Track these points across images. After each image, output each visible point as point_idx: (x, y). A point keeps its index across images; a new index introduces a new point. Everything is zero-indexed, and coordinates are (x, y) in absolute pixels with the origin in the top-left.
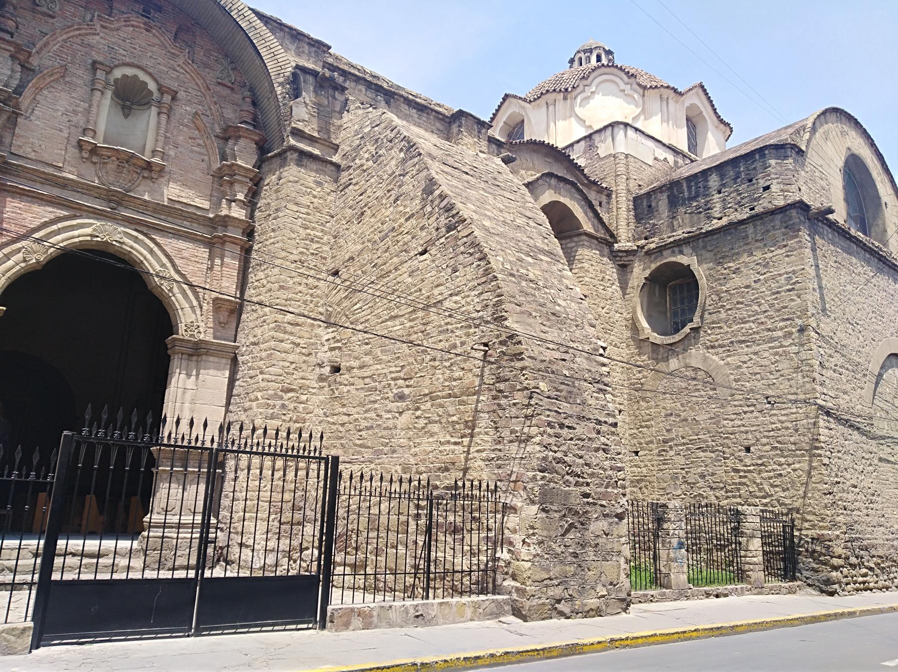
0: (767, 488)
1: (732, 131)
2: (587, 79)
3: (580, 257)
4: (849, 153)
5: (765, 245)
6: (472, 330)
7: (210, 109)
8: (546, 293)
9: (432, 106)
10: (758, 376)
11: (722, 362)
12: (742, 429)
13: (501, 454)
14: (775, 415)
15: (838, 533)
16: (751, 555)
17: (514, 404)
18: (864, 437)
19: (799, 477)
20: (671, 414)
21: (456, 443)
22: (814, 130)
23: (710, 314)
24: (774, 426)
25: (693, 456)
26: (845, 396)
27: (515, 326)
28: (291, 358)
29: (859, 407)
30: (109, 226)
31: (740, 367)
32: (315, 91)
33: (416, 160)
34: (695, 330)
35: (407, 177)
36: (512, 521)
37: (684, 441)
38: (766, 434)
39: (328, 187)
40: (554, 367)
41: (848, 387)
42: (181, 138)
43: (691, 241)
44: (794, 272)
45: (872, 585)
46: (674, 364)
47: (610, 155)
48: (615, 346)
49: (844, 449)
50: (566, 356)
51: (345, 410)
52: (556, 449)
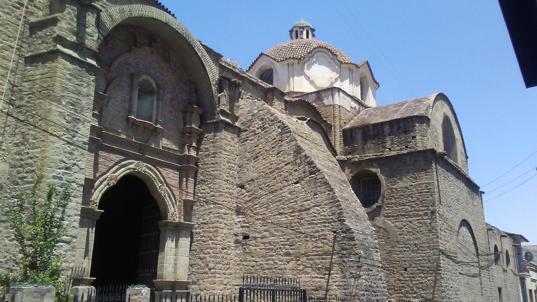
0: (415, 289)
5: (415, 168)
6: (327, 225)
7: (177, 96)
11: (393, 225)
12: (403, 259)
13: (346, 283)
14: (419, 253)
21: (321, 278)
22: (433, 106)
23: (387, 199)
27: (349, 224)
28: (225, 231)
30: (141, 163)
31: (402, 228)
32: (229, 89)
33: (289, 134)
34: (379, 207)
35: (284, 142)
39: (236, 140)
40: (364, 243)
42: (166, 112)
43: (380, 161)
44: (429, 183)
51: (254, 259)
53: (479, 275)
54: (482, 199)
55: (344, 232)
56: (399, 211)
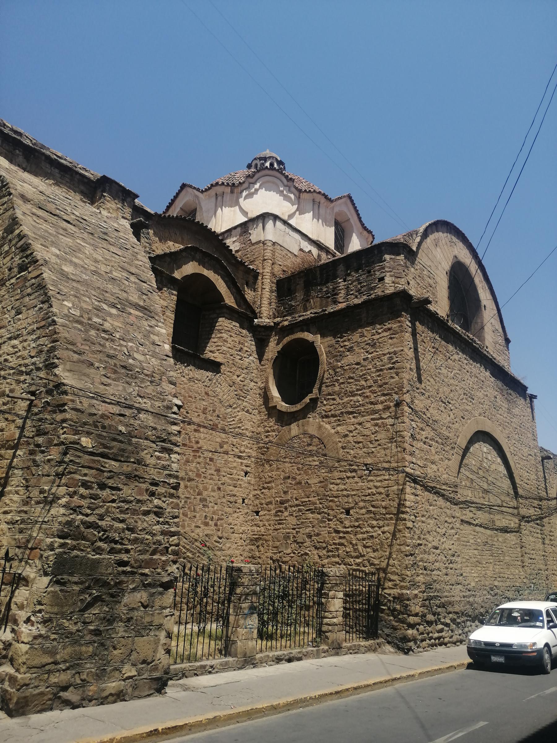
0: (360, 548)
1: (374, 238)
2: (252, 178)
3: (220, 328)
4: (455, 260)
6: (22, 378)
8: (121, 345)
9: (77, 169)
10: (361, 444)
11: (333, 431)
12: (345, 493)
14: (372, 481)
15: (416, 592)
16: (330, 616)
17: (49, 461)
18: (448, 503)
19: (387, 539)
20: (289, 477)
22: (425, 235)
23: (327, 386)
24: (370, 491)
25: (303, 517)
26: (434, 466)
29: (445, 476)
31: (346, 436)
33: (6, 199)
34: (314, 401)
36: (22, 594)
37: (296, 502)
38: (363, 498)
40: (107, 423)
41: (436, 458)
44: (395, 353)
45: (446, 640)
46: (295, 429)
47: (259, 242)
48: (248, 411)
49: (428, 514)
50: (128, 412)
52: (89, 511)
53: (518, 531)
54: (532, 408)
55: (49, 392)
56: (344, 405)
